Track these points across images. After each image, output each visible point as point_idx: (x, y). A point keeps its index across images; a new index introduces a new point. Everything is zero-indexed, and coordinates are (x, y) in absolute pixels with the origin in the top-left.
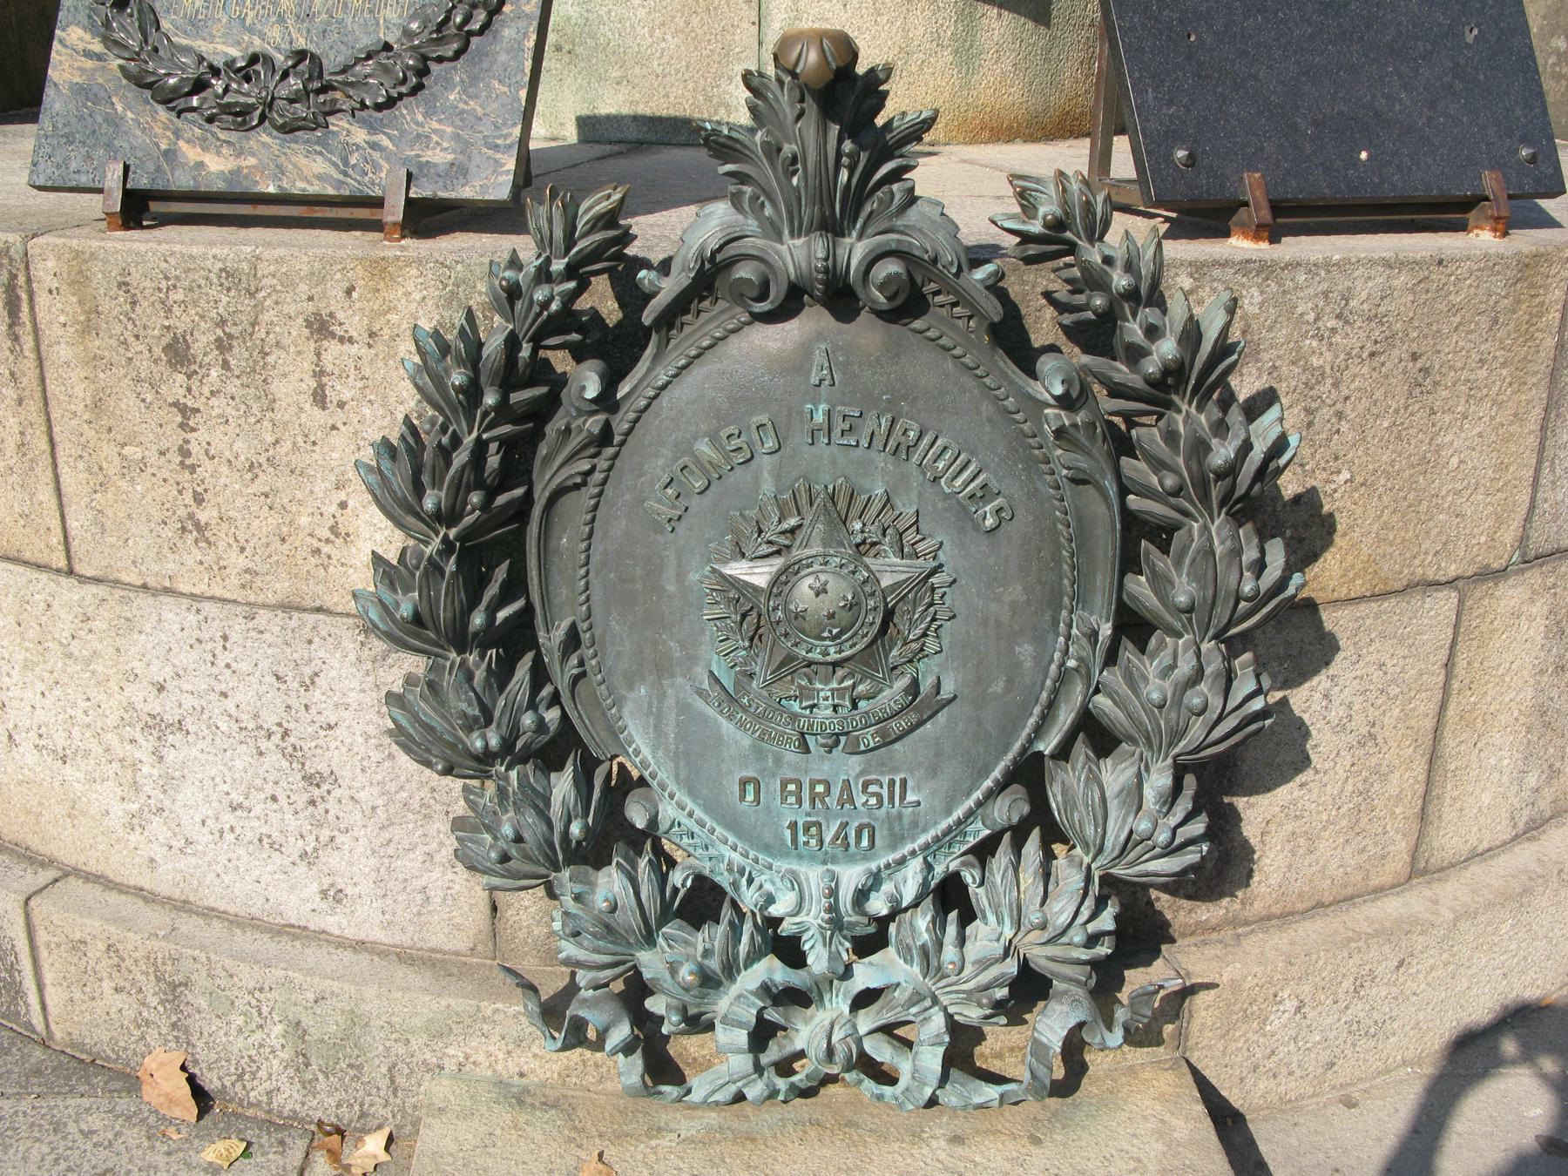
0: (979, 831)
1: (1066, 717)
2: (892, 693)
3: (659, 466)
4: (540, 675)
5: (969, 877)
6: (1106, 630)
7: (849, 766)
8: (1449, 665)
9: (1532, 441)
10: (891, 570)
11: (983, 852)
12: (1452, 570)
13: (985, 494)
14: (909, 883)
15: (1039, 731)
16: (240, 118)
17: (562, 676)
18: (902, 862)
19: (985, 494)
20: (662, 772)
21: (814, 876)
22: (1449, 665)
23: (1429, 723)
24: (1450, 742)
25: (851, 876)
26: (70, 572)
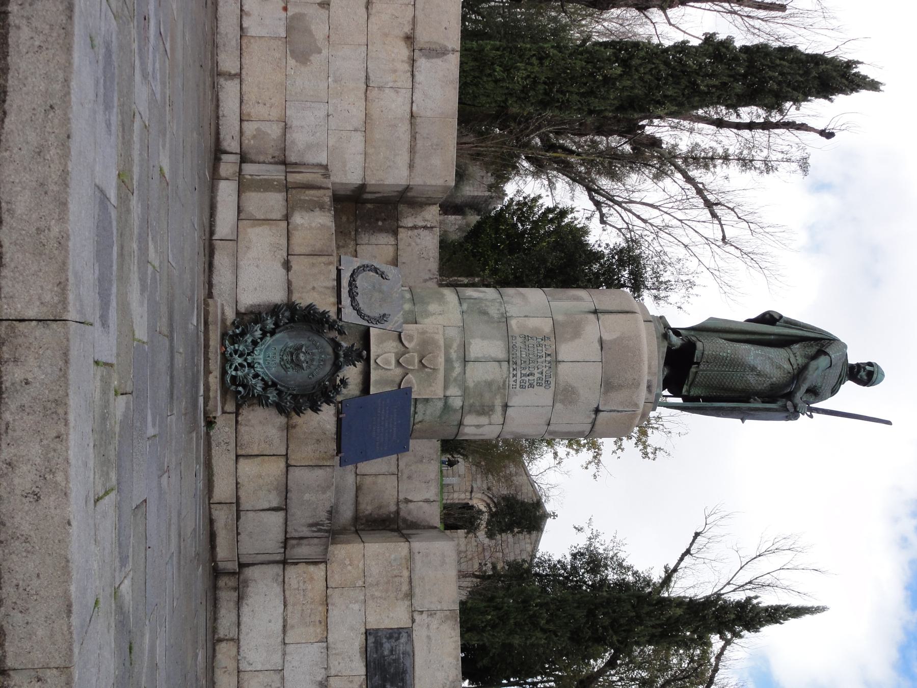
0: (266, 378)
1: (283, 388)
2: (288, 366)
3: (316, 338)
4: (287, 323)
5: (260, 378)
6: (295, 392)
7: (278, 360)
8: (274, 455)
9: (307, 464)
10: (304, 365)
11: (263, 380)
12: (289, 452)
13: (313, 376)
14: (258, 369)
15: (281, 385)
16: (350, 284)
17: (287, 326)
18: (262, 368)
19: (313, 376)
20: (274, 338)
21: (261, 356)
22: (274, 455)
23: (265, 453)
24: (260, 458)
25: (261, 361)
26: (288, 255)
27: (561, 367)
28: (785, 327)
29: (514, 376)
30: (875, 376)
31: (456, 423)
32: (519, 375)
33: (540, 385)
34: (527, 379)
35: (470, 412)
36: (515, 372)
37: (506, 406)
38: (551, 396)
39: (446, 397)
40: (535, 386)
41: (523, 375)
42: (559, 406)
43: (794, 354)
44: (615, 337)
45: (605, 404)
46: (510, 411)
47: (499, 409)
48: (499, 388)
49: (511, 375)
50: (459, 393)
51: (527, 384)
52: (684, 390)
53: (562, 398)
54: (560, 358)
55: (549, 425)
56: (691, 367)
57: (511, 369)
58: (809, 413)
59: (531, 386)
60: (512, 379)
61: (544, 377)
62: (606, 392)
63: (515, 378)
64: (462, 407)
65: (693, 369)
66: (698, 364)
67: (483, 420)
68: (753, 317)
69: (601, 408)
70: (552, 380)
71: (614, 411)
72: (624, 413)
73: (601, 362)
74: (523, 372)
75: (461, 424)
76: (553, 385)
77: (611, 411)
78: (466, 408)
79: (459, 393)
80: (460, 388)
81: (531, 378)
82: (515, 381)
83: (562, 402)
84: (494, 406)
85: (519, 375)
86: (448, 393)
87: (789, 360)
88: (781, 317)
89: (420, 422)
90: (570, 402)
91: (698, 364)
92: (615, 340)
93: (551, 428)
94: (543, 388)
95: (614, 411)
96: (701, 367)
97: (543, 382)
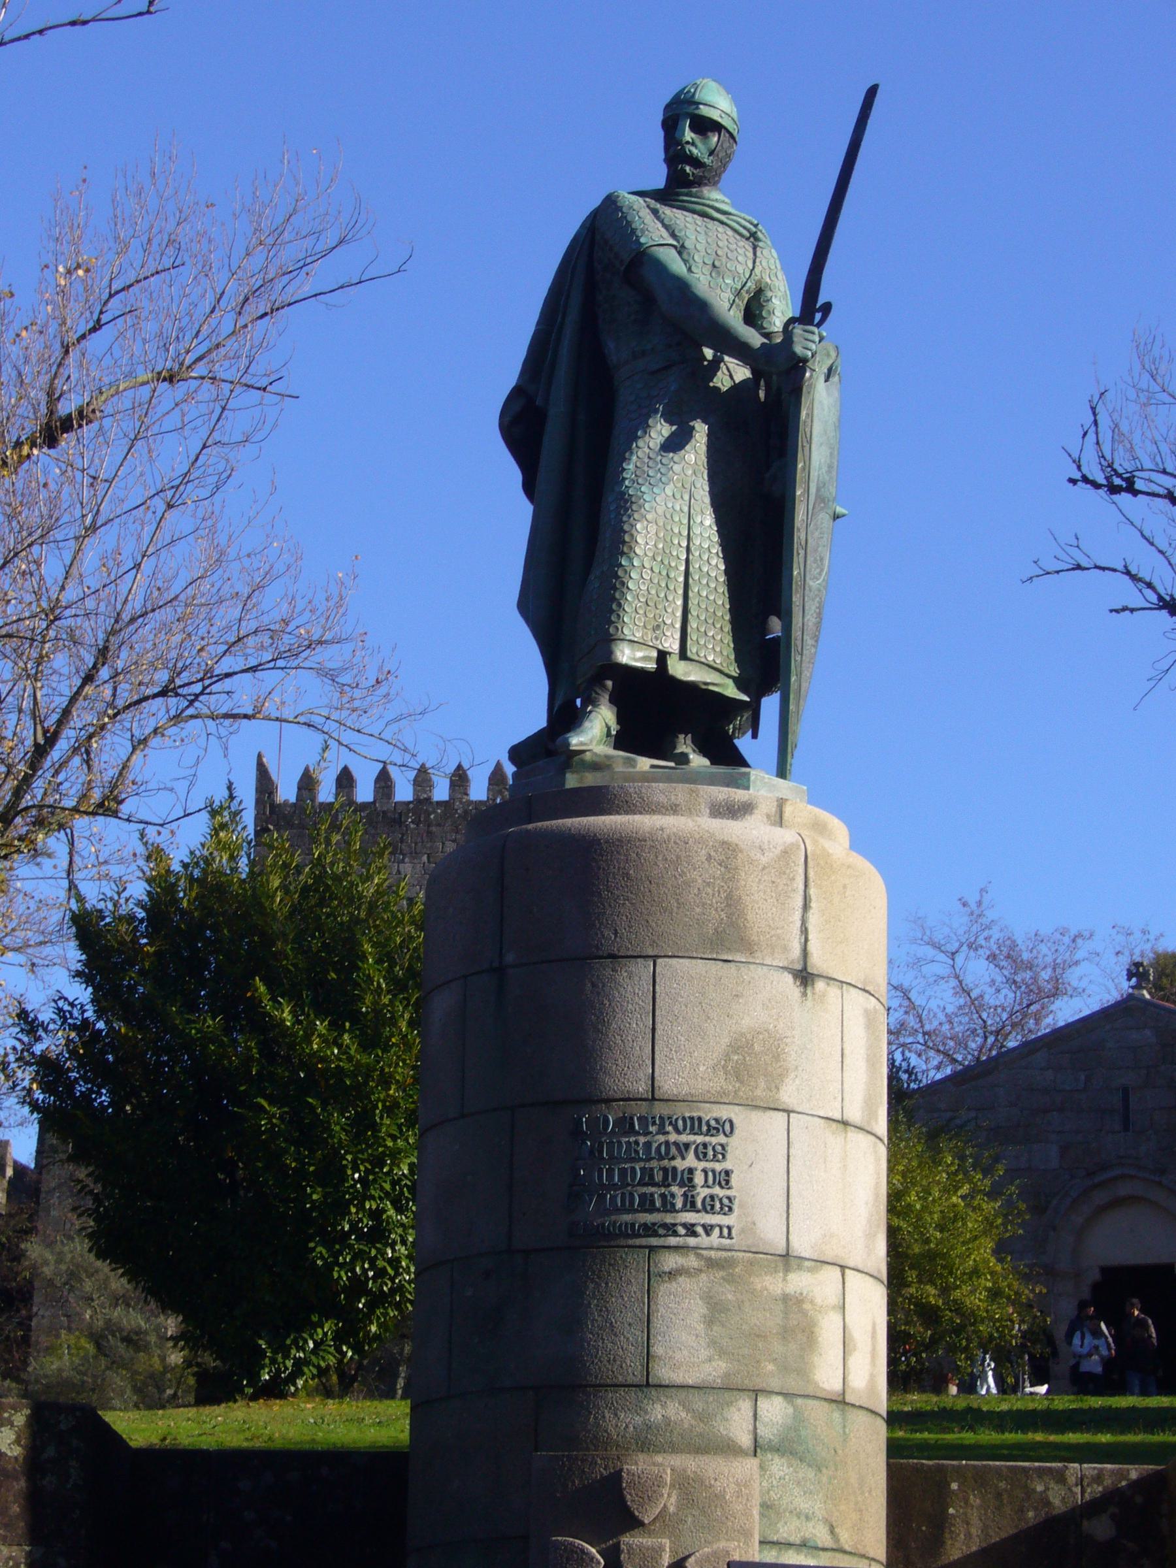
27: (668, 1084)
29: (691, 1230)
30: (705, 111)
31: (836, 1415)
32: (690, 1217)
33: (721, 1153)
34: (702, 1193)
35: (803, 1370)
36: (682, 1231)
37: (787, 1259)
38: (755, 1115)
39: (757, 1447)
40: (728, 1165)
41: (690, 1204)
42: (788, 1094)
45: (785, 949)
46: (802, 1245)
47: (798, 1282)
48: (730, 1279)
49: (692, 1241)
50: (745, 1405)
51: (717, 1190)
53: (762, 1085)
54: (642, 1088)
55: (845, 1123)
56: (674, 680)
57: (673, 1241)
58: (818, 316)
59: (724, 1179)
60: (703, 1240)
61: (699, 1139)
62: (748, 946)
63: (699, 1230)
64: (787, 1395)
65: (679, 670)
66: (662, 656)
67: (829, 1330)
68: (515, 475)
70: (709, 1113)
71: (804, 922)
72: (812, 891)
74: (679, 1204)
75: (840, 1401)
76: (724, 1113)
77: (805, 931)
78: (792, 1383)
79: (745, 1405)
80: (729, 1404)
81: (699, 1179)
82: (708, 1229)
83: (776, 1082)
84: (786, 1298)
85: (690, 1217)
86: (745, 1440)
88: (517, 393)
89: (832, 1531)
90: (777, 1058)
93: (854, 1114)
94: (734, 1143)
95: (804, 922)
97: (714, 1140)
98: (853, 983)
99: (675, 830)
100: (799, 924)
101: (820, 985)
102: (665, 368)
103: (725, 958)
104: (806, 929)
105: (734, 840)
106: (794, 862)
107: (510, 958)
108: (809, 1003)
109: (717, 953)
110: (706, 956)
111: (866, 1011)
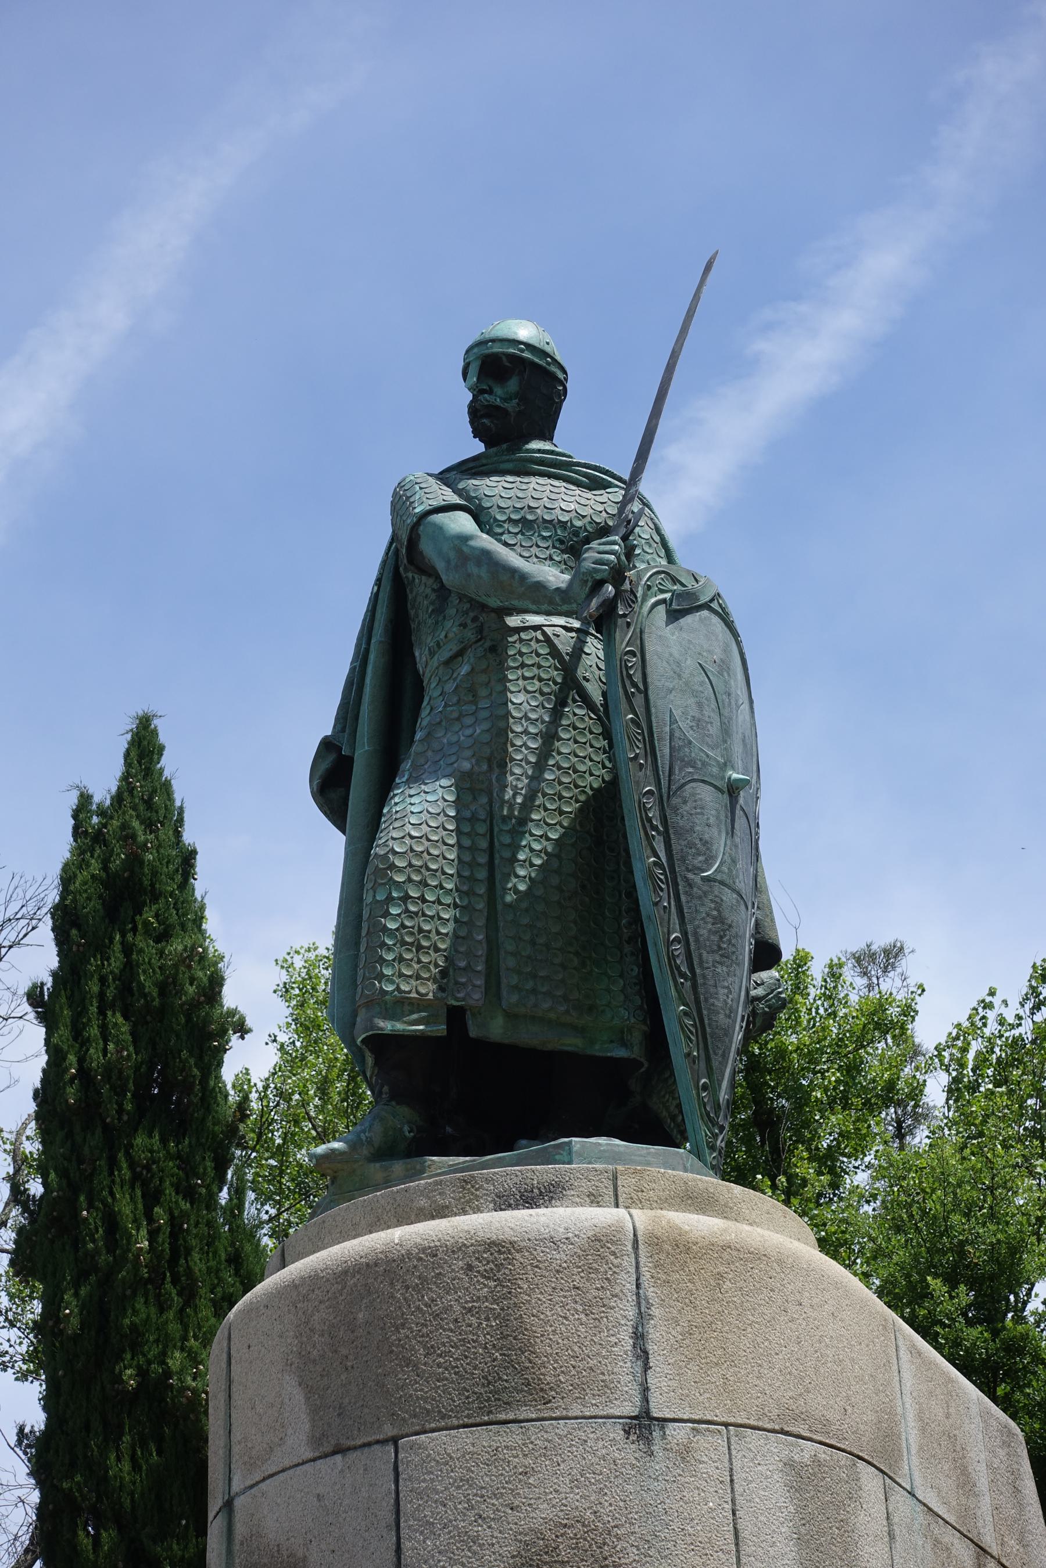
28: (356, 718)
43: (432, 654)
44: (298, 1396)
52: (621, 1053)
66: (456, 1016)
69: (630, 1408)
71: (639, 1337)
72: (650, 1291)
73: (395, 1440)
77: (643, 1355)
87: (448, 662)
88: (326, 745)
91: (456, 1016)
92: (309, 1391)
95: (639, 1337)
96: (474, 996)
98: (752, 1422)
99: (418, 1240)
100: (628, 1343)
101: (677, 1433)
102: (460, 653)
103: (502, 1416)
104: (646, 1352)
105: (508, 1235)
106: (614, 1254)
107: (236, 1486)
108: (658, 1466)
109: (490, 1412)
110: (471, 1421)
111: (789, 1464)
